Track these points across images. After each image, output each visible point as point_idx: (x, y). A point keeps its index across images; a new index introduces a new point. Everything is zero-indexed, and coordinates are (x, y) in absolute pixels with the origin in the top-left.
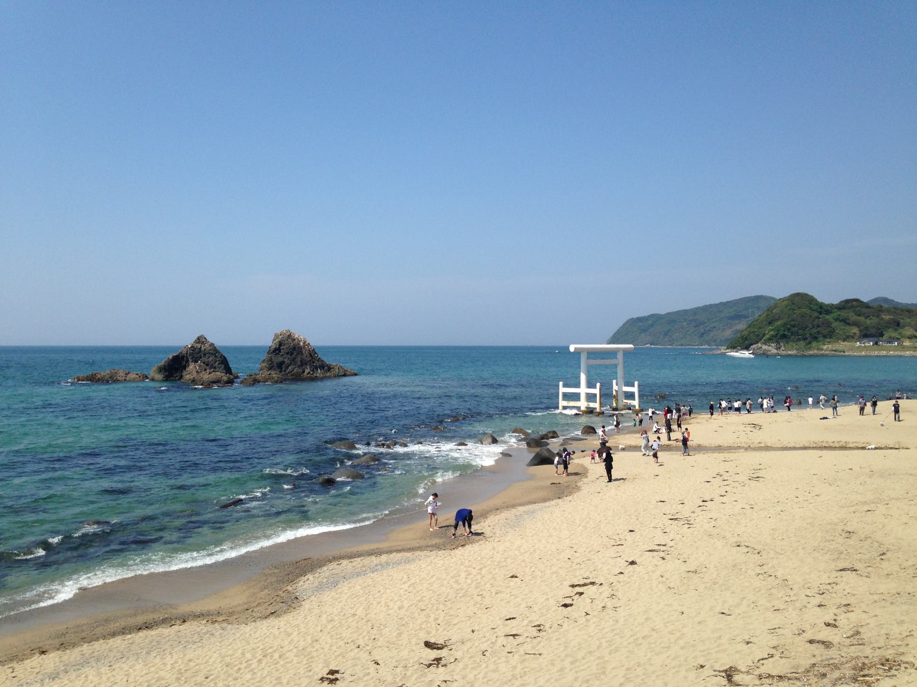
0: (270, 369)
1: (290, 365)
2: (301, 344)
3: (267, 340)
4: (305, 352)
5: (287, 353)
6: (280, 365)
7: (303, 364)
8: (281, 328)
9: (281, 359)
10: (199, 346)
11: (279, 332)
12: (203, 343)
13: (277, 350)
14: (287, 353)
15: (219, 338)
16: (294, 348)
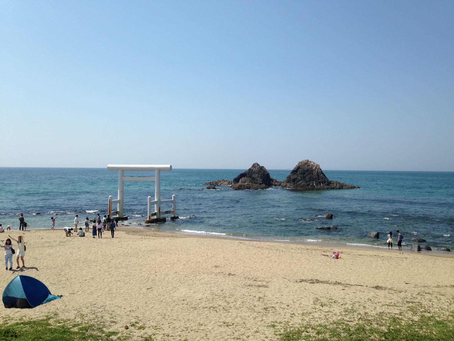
0: (288, 182)
1: (301, 180)
2: (314, 168)
3: (292, 166)
4: (315, 173)
5: (301, 174)
6: (294, 180)
7: (311, 179)
8: (302, 158)
9: (296, 177)
10: (252, 168)
11: (301, 161)
12: (255, 167)
13: (294, 172)
14: (301, 174)
15: (269, 166)
16: (308, 171)
